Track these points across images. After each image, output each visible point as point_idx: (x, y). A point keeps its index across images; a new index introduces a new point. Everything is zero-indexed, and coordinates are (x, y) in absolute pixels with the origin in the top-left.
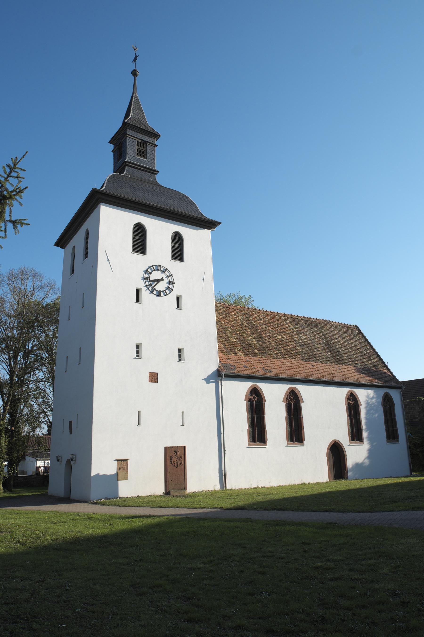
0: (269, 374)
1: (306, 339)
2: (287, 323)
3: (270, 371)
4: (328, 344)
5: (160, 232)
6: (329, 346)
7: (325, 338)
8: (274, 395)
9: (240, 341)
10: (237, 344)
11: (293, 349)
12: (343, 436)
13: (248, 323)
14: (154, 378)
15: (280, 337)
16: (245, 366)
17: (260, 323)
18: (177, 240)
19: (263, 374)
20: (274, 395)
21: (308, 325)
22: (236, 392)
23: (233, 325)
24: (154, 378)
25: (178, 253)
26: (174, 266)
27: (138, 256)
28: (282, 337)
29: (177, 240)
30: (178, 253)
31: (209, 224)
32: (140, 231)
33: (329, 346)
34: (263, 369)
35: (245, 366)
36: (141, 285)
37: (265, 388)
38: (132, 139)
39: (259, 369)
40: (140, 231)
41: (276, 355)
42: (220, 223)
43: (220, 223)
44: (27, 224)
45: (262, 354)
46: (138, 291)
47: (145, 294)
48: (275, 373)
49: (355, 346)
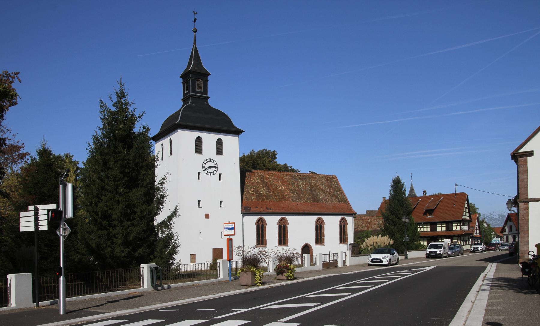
0: (270, 211)
1: (298, 187)
2: (286, 178)
3: (271, 209)
4: (311, 189)
5: (209, 139)
6: (312, 191)
7: (311, 186)
8: (272, 223)
9: (255, 192)
10: (253, 195)
11: (286, 195)
12: (311, 241)
13: (262, 181)
14: (207, 216)
15: (280, 188)
16: (256, 207)
17: (269, 180)
18: (219, 143)
19: (266, 211)
20: (272, 223)
21: (300, 178)
22: (252, 220)
23: (252, 183)
24: (207, 216)
25: (220, 151)
26: (218, 159)
27: (199, 155)
28: (282, 188)
29: (219, 143)
30: (220, 151)
31: (237, 132)
32: (199, 141)
33: (312, 191)
34: (267, 208)
35: (256, 207)
36: (201, 170)
37: (267, 218)
38: (195, 77)
39: (264, 209)
40: (199, 141)
41: (276, 199)
42: (242, 131)
43: (242, 131)
44: (174, 214)
45: (268, 199)
46: (199, 173)
47: (203, 174)
48: (273, 210)
49: (330, 189)
